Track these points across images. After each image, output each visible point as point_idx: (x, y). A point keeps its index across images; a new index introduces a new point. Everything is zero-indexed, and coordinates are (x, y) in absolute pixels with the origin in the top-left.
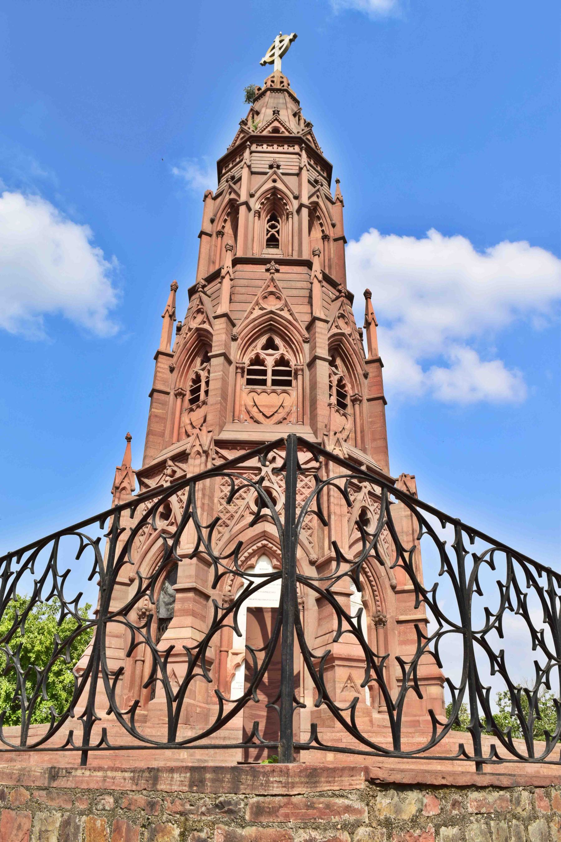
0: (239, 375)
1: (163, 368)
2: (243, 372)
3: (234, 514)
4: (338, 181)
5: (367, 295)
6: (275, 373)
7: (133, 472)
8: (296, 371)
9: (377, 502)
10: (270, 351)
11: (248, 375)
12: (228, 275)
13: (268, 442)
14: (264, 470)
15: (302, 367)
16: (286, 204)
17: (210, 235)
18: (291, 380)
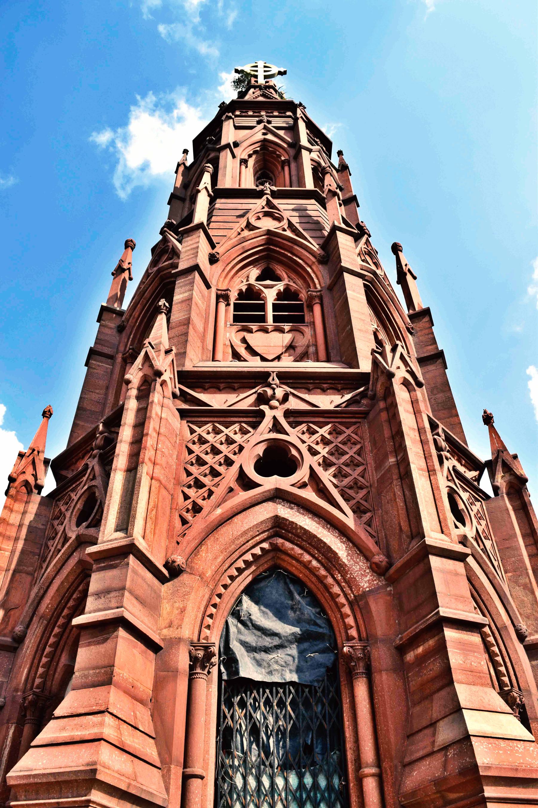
0: (222, 306)
1: (111, 328)
2: (228, 305)
3: (213, 489)
4: (340, 153)
5: (396, 249)
6: (276, 307)
7: (46, 462)
8: (310, 299)
9: (467, 491)
10: (268, 282)
11: (234, 312)
12: (204, 189)
13: (273, 372)
14: (269, 413)
15: (319, 293)
16: (280, 156)
17: (183, 200)
18: (303, 316)
